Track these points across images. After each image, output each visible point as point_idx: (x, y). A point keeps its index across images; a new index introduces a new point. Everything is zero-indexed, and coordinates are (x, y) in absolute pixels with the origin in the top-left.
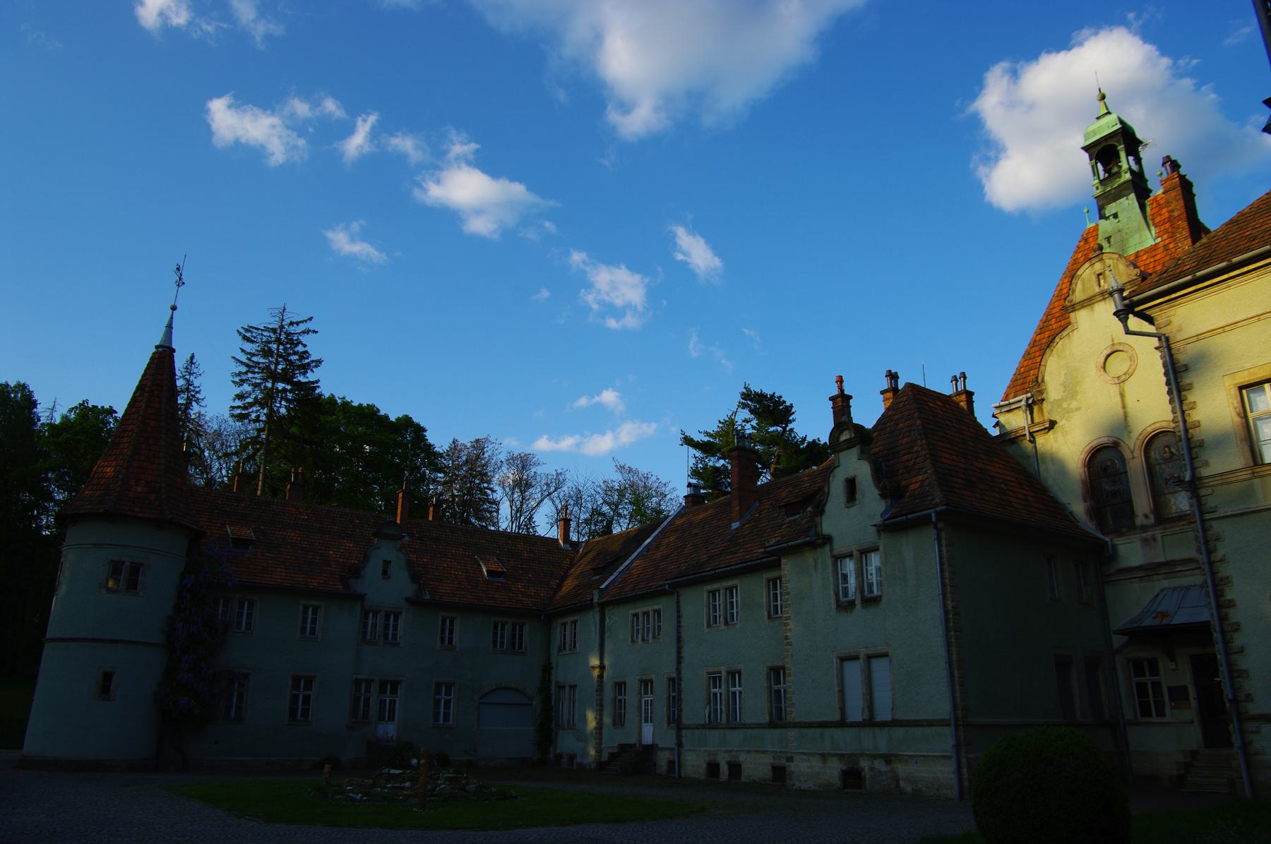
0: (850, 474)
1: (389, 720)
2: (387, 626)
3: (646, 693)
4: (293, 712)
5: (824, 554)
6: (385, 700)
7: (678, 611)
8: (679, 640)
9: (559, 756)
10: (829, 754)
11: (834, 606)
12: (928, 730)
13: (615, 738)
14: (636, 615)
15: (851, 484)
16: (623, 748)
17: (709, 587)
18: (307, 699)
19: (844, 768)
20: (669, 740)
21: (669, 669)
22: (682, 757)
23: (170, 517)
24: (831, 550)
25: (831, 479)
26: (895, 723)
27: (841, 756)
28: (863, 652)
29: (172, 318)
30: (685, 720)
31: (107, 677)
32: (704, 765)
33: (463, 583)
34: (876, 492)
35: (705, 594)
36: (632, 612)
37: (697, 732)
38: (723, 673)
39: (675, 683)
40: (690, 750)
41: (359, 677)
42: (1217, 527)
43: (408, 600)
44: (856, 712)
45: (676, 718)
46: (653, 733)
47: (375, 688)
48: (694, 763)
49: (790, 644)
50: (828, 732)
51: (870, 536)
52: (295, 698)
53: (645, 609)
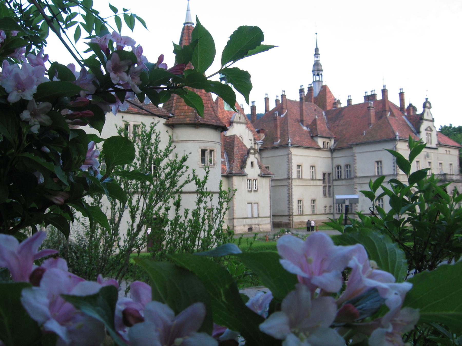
0: (252, 161)
5: (245, 178)
10: (246, 225)
11: (247, 191)
12: (265, 218)
15: (252, 163)
19: (249, 227)
24: (247, 177)
25: (248, 160)
26: (259, 217)
27: (248, 225)
28: (253, 202)
29: (188, 5)
34: (259, 168)
42: (293, 187)
44: (255, 215)
49: (235, 199)
50: (244, 220)
51: (256, 177)
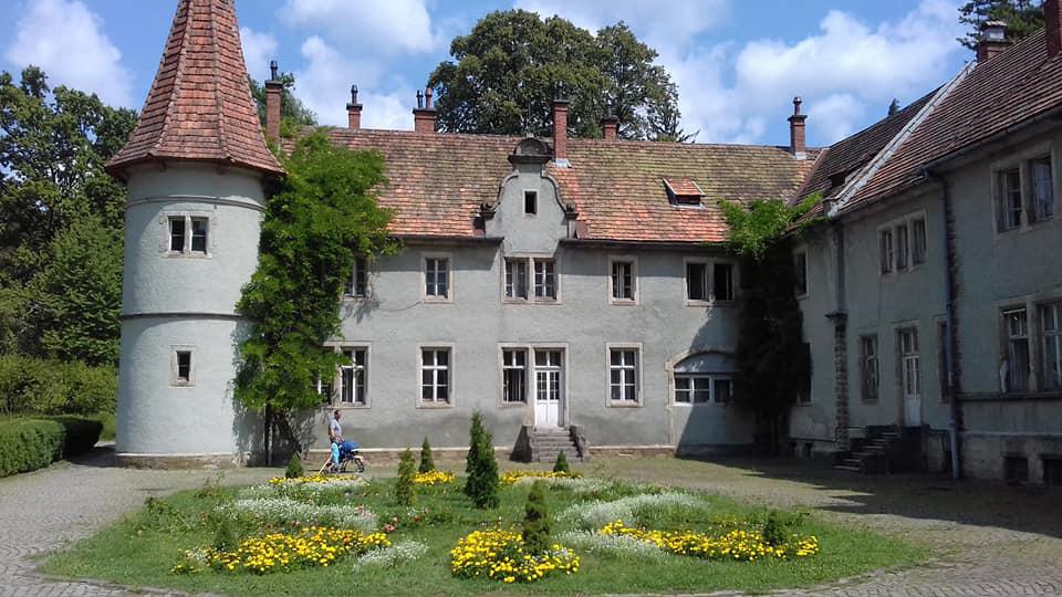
1: (552, 398)
2: (539, 279)
3: (907, 350)
4: (427, 393)
6: (545, 374)
7: (948, 213)
8: (951, 259)
9: (793, 443)
13: (865, 416)
14: (886, 233)
16: (875, 432)
17: (1000, 164)
18: (443, 376)
20: (941, 419)
21: (939, 308)
22: (964, 446)
23: (228, 155)
30: (969, 386)
31: (184, 359)
32: (1001, 461)
33: (641, 215)
35: (993, 178)
36: (881, 227)
37: (989, 408)
38: (1028, 306)
39: (950, 330)
40: (975, 436)
41: (506, 345)
43: (562, 243)
45: (950, 384)
46: (921, 408)
47: (532, 356)
48: (984, 455)
52: (427, 376)
53: (899, 221)
